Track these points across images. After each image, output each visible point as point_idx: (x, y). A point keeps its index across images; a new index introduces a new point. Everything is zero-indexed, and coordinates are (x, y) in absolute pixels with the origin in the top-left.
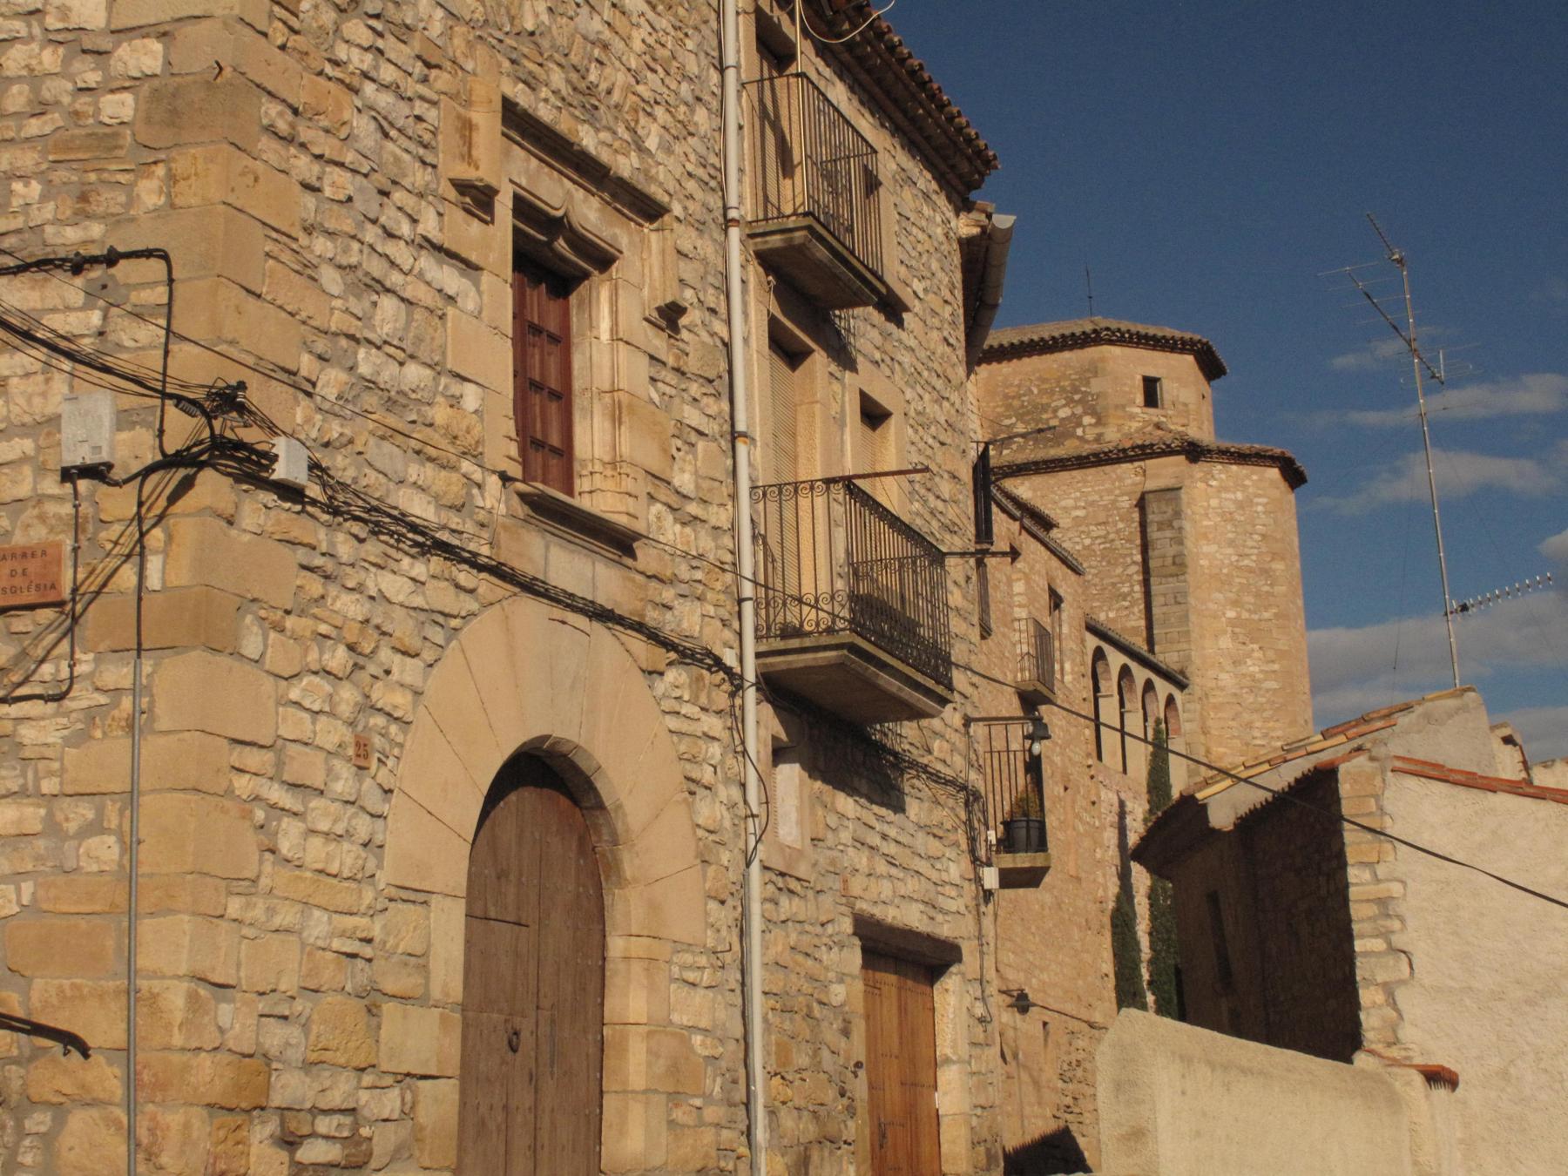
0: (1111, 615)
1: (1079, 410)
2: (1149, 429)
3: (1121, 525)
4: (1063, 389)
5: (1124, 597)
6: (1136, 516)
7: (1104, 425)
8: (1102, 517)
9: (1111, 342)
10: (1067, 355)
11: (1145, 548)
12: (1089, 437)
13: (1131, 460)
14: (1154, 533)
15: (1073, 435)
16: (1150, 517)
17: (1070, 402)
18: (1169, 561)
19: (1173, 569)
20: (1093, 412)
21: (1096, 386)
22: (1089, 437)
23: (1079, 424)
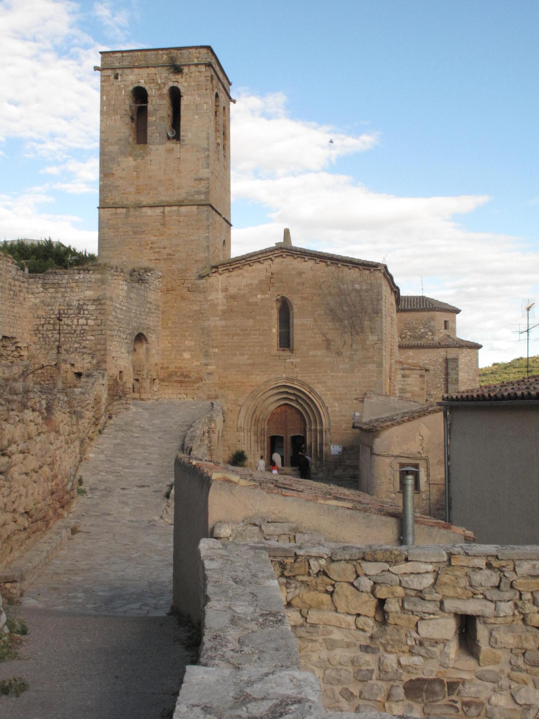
0: (435, 392)
1: (427, 330)
2: (445, 337)
3: (439, 367)
4: (422, 323)
5: (439, 388)
6: (444, 364)
7: (435, 336)
8: (433, 363)
9: (438, 311)
10: (424, 313)
11: (447, 374)
12: (430, 338)
13: (444, 348)
14: (450, 371)
15: (425, 337)
16: (449, 366)
17: (424, 327)
18: (454, 379)
19: (455, 382)
20: (431, 331)
21: (432, 323)
22: (430, 338)
23: (427, 334)
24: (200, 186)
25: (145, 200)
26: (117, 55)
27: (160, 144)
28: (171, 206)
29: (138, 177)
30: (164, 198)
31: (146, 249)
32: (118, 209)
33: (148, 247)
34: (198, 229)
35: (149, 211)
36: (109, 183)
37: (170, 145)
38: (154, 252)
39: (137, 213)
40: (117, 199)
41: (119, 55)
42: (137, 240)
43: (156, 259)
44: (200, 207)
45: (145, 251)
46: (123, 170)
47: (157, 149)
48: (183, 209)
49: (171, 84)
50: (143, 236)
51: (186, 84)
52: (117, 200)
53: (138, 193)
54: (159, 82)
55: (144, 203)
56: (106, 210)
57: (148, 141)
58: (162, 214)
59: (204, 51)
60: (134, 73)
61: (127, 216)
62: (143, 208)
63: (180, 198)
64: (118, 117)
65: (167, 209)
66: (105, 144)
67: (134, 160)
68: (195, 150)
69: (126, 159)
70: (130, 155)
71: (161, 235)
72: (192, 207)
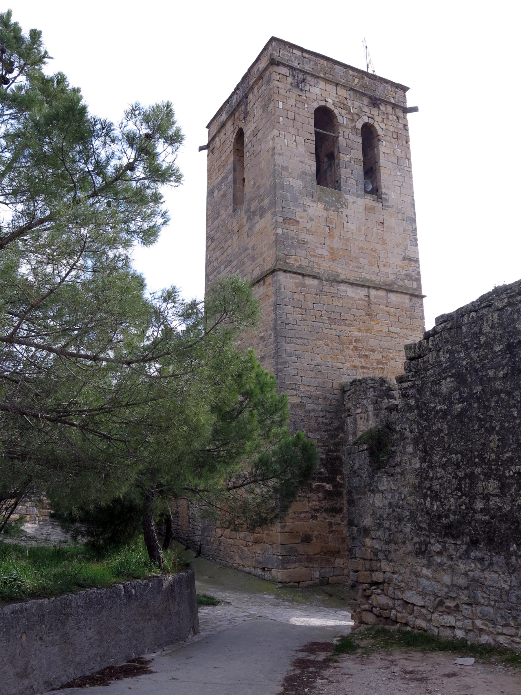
24: (410, 269)
25: (344, 273)
26: (295, 51)
27: (358, 196)
28: (376, 288)
29: (331, 236)
30: (368, 277)
31: (348, 348)
32: (306, 278)
33: (351, 347)
34: (412, 330)
35: (350, 291)
36: (292, 234)
37: (369, 200)
38: (360, 356)
39: (333, 290)
40: (305, 262)
41: (299, 53)
42: (334, 332)
43: (363, 367)
44: (413, 298)
45: (347, 352)
46: (311, 219)
47: (354, 202)
48: (393, 297)
49: (366, 119)
50: (343, 328)
51: (383, 126)
52: (304, 264)
53: (334, 260)
54: (352, 111)
55: (342, 277)
56: (288, 275)
57: (343, 188)
58: (367, 299)
59: (400, 92)
60: (320, 86)
61: (320, 293)
62: (341, 284)
63: (389, 280)
64: (300, 139)
65: (373, 292)
66: (283, 173)
67: (326, 210)
68: (400, 218)
69: (315, 205)
70: (319, 200)
71: (368, 330)
72: (403, 296)
